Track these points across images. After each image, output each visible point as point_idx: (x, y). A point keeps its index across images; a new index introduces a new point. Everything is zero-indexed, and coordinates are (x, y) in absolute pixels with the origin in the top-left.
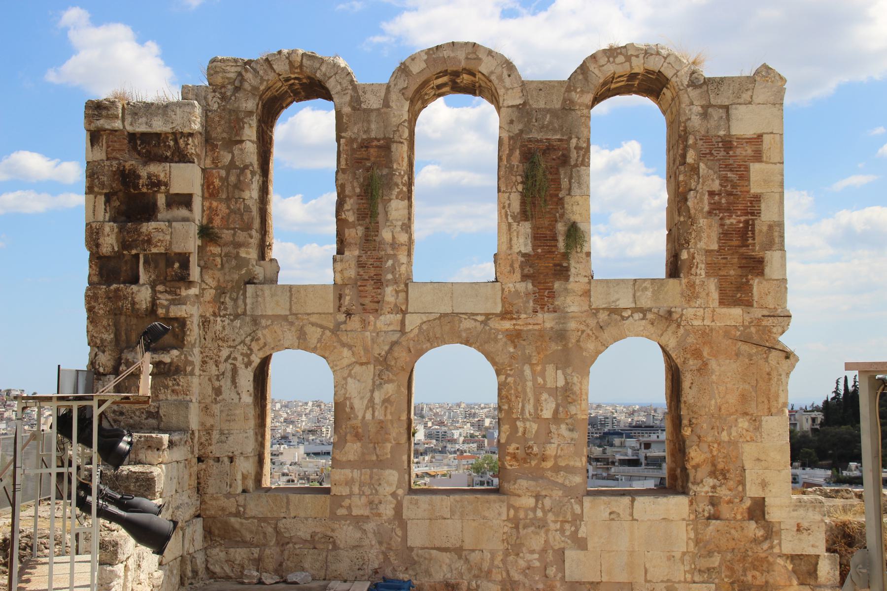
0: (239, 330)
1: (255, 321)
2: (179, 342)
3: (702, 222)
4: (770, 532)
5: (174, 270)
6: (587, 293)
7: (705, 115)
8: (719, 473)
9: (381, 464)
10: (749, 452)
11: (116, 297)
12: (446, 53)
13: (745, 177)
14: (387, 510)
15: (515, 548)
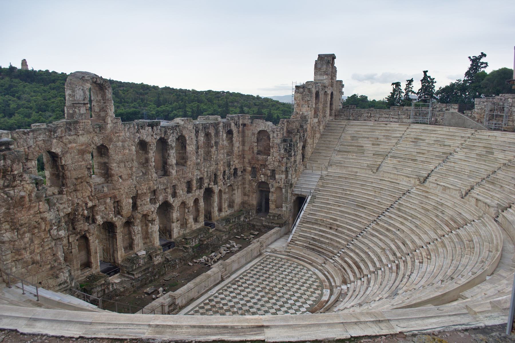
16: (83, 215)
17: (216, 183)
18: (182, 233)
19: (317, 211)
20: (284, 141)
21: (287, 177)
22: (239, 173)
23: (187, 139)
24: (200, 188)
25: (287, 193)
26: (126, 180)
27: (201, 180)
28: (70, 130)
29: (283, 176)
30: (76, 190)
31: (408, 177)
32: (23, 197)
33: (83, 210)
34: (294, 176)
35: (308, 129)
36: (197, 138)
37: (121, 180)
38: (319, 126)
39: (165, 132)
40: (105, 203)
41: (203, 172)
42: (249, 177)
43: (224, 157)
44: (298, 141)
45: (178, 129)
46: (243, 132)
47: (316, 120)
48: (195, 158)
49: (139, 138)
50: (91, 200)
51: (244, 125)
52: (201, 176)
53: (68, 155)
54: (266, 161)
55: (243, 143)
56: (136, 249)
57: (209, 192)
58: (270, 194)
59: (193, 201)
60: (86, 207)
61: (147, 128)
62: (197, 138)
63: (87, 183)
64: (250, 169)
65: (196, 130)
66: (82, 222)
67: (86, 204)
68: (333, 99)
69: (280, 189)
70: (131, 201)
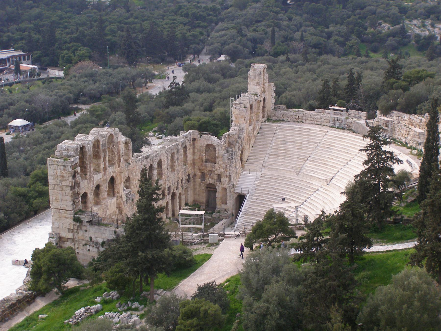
4: (122, 200)
17: (177, 188)
19: (254, 206)
20: (227, 152)
21: (230, 180)
23: (163, 161)
24: (169, 194)
25: (231, 192)
27: (169, 188)
29: (227, 179)
31: (320, 178)
34: (235, 178)
35: (245, 139)
38: (253, 131)
42: (198, 180)
44: (238, 150)
46: (194, 144)
47: (251, 128)
51: (194, 140)
54: (213, 168)
55: (194, 153)
57: (174, 195)
58: (217, 193)
64: (200, 174)
68: (266, 103)
69: (225, 189)
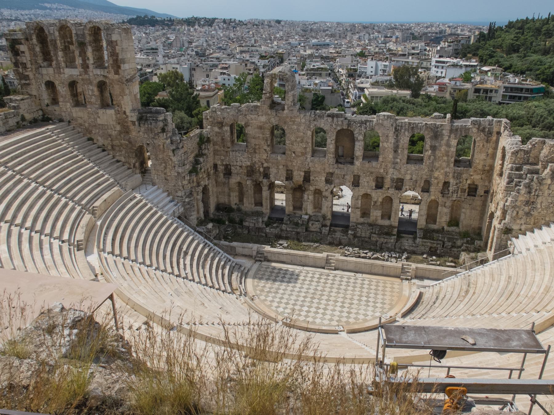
0: (40, 76)
1: (42, 75)
2: (29, 80)
3: (110, 58)
4: (127, 117)
5: (24, 66)
6: (92, 72)
7: (107, 36)
8: (118, 106)
9: (67, 102)
10: (122, 102)
11: (17, 70)
12: (62, 22)
13: (115, 49)
14: (69, 110)
15: (89, 118)
16: (259, 170)
18: (362, 220)
20: (519, 169)
22: (481, 191)
23: (380, 135)
26: (298, 156)
28: (252, 111)
30: (255, 152)
32: (159, 145)
33: (259, 167)
36: (397, 136)
37: (294, 155)
39: (349, 125)
40: (278, 169)
41: (403, 173)
43: (448, 165)
45: (368, 124)
46: (497, 142)
48: (391, 156)
49: (315, 125)
50: (267, 162)
52: (400, 176)
53: (249, 128)
56: (304, 212)
59: (382, 197)
60: (263, 167)
61: (325, 118)
62: (397, 136)
63: (265, 150)
65: (396, 128)
66: (258, 174)
67: (262, 164)
70: (303, 174)
